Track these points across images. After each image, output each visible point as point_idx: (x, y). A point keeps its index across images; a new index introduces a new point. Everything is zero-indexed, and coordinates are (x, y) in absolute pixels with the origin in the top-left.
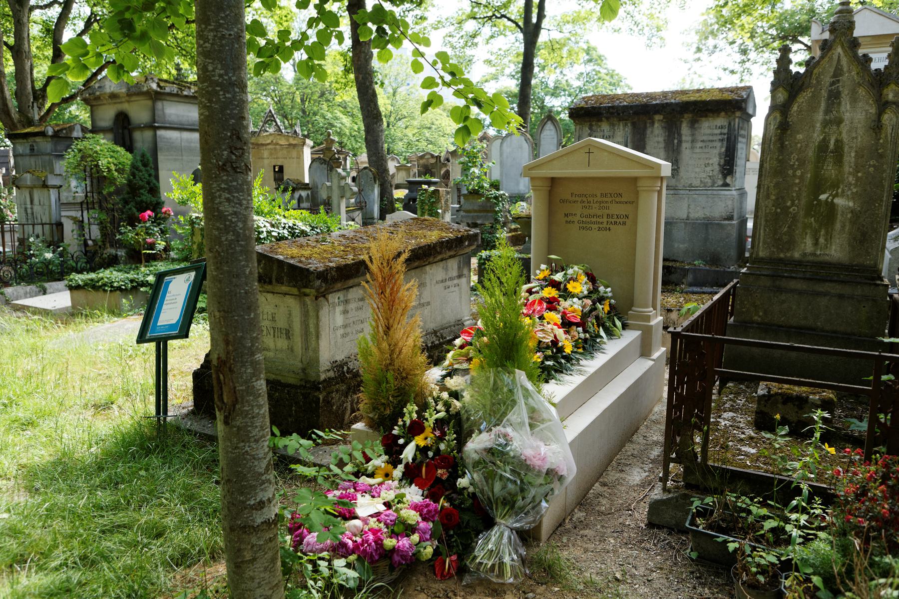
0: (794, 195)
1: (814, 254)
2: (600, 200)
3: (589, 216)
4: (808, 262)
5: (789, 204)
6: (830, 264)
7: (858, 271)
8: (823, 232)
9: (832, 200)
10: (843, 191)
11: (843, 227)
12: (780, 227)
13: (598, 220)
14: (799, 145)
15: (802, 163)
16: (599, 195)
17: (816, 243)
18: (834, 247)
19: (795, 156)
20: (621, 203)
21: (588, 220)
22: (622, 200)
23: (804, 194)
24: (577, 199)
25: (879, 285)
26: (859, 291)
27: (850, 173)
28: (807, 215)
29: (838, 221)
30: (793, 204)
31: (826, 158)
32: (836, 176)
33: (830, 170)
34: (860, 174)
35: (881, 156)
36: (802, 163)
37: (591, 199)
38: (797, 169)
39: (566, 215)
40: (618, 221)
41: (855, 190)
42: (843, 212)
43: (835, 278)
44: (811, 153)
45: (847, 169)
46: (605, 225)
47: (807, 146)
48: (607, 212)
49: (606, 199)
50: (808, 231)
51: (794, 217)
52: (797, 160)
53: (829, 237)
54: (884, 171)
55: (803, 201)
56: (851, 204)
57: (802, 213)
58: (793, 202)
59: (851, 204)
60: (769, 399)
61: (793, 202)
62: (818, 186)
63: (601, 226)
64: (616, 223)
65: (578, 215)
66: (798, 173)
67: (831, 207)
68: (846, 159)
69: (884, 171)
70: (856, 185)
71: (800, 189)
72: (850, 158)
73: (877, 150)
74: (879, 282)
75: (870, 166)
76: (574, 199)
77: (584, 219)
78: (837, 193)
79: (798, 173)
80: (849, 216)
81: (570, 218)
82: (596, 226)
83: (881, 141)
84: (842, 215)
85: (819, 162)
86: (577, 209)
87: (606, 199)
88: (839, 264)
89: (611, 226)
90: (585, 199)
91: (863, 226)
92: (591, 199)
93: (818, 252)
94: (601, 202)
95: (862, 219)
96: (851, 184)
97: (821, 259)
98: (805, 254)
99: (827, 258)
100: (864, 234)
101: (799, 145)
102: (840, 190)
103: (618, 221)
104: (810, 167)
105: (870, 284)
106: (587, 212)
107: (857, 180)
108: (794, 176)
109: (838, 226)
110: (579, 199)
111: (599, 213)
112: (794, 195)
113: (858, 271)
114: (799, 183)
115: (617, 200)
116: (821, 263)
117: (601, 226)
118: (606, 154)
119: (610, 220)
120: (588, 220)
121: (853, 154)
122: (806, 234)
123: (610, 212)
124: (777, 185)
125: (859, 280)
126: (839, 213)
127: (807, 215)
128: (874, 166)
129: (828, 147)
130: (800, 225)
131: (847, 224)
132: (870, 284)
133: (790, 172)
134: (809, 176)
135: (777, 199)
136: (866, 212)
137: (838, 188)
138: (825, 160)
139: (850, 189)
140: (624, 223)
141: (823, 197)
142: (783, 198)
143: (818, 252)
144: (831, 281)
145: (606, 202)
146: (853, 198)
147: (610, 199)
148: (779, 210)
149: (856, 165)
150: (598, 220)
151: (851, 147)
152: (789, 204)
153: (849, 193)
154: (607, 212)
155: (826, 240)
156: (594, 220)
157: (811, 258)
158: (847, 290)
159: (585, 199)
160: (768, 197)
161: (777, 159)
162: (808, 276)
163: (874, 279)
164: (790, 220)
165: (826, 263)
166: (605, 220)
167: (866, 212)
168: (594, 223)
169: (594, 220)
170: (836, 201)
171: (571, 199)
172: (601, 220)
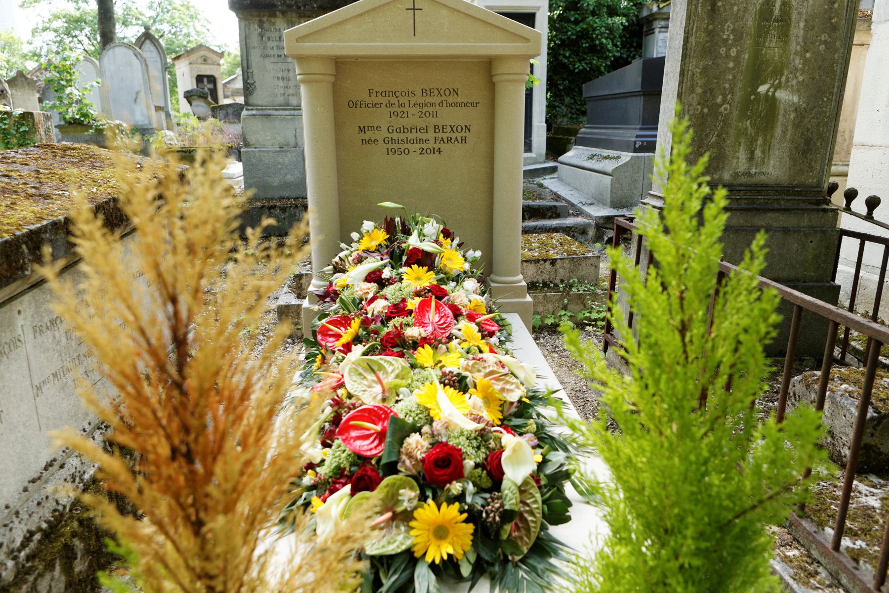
0: (727, 86)
1: (748, 174)
2: (421, 100)
3: (403, 130)
4: (741, 185)
5: (719, 100)
6: (767, 186)
7: (799, 193)
8: (760, 142)
9: (774, 94)
10: (787, 81)
11: (784, 133)
12: (707, 136)
13: (420, 135)
14: (736, 8)
15: (739, 35)
16: (418, 92)
17: (751, 158)
18: (772, 162)
19: (729, 25)
20: (456, 105)
21: (402, 136)
22: (459, 100)
23: (740, 85)
24: (380, 99)
25: (825, 210)
26: (805, 221)
27: (796, 53)
28: (743, 116)
29: (779, 123)
30: (724, 101)
31: (769, 29)
32: (781, 56)
33: (773, 49)
34: (808, 55)
35: (834, 28)
36: (739, 35)
37: (404, 100)
38: (732, 46)
39: (362, 130)
40: (453, 136)
41: (801, 78)
42: (785, 111)
43: (776, 206)
44: (750, 22)
45: (794, 47)
46: (431, 144)
47: (746, 9)
48: (434, 121)
49: (429, 99)
50: (742, 140)
51: (726, 122)
52: (733, 31)
53: (767, 149)
54: (836, 50)
55: (738, 95)
56: (796, 99)
57: (735, 113)
58: (725, 96)
59: (796, 99)
60: (879, 424)
61: (725, 96)
62: (757, 75)
63: (425, 146)
64: (449, 140)
65: (384, 128)
66: (733, 52)
67: (772, 102)
68: (793, 31)
69: (836, 50)
70: (803, 71)
71: (734, 77)
72: (798, 30)
73: (831, 18)
74: (826, 207)
75: (821, 42)
76: (374, 99)
77: (395, 136)
78: (780, 83)
79: (733, 52)
80: (792, 116)
81: (369, 135)
82: (417, 147)
83: (836, 6)
84: (784, 116)
85: (759, 36)
86: (382, 118)
87: (429, 99)
88: (779, 185)
89: (442, 146)
90: (393, 100)
91: (808, 129)
92: (404, 100)
93: (753, 171)
94: (422, 105)
95: (807, 120)
96: (796, 69)
97: (755, 180)
98: (737, 174)
99: (763, 178)
100: (808, 142)
101: (736, 8)
102: (783, 79)
103: (453, 136)
104: (748, 42)
105: (818, 210)
106: (398, 122)
107: (804, 64)
108: (728, 56)
109: (778, 131)
110: (384, 101)
111: (421, 123)
112: (727, 86)
113: (799, 193)
114: (733, 69)
115: (451, 100)
116: (756, 185)
117: (425, 146)
118: (445, 12)
119: (440, 135)
120: (402, 136)
121: (802, 25)
122: (740, 144)
123: (439, 121)
124: (705, 70)
125: (802, 206)
126: (781, 112)
127: (743, 116)
128: (825, 43)
129: (772, 12)
130: (732, 132)
131: (790, 127)
132: (818, 210)
133: (723, 51)
134: (747, 56)
135: (705, 92)
136: (812, 110)
137: (782, 75)
138: (767, 33)
139: (796, 77)
140: (464, 140)
141: (762, 89)
142: (712, 91)
143: (753, 171)
144: (773, 210)
145: (432, 104)
146: (798, 90)
147: (438, 100)
148: (706, 110)
149: (805, 38)
150: (420, 135)
151: (800, 14)
152: (719, 100)
153: (794, 82)
154: (434, 121)
155: (763, 152)
156: (411, 136)
157: (743, 180)
158: (790, 221)
159: (393, 100)
160: (692, 90)
161: (706, 30)
162: (744, 206)
163: (818, 203)
164: (720, 125)
165: (762, 186)
166: (431, 135)
167: (812, 110)
168: (413, 141)
169: (411, 136)
170: (778, 94)
171: (369, 100)
172: (424, 136)
